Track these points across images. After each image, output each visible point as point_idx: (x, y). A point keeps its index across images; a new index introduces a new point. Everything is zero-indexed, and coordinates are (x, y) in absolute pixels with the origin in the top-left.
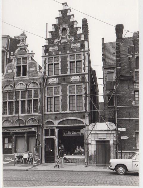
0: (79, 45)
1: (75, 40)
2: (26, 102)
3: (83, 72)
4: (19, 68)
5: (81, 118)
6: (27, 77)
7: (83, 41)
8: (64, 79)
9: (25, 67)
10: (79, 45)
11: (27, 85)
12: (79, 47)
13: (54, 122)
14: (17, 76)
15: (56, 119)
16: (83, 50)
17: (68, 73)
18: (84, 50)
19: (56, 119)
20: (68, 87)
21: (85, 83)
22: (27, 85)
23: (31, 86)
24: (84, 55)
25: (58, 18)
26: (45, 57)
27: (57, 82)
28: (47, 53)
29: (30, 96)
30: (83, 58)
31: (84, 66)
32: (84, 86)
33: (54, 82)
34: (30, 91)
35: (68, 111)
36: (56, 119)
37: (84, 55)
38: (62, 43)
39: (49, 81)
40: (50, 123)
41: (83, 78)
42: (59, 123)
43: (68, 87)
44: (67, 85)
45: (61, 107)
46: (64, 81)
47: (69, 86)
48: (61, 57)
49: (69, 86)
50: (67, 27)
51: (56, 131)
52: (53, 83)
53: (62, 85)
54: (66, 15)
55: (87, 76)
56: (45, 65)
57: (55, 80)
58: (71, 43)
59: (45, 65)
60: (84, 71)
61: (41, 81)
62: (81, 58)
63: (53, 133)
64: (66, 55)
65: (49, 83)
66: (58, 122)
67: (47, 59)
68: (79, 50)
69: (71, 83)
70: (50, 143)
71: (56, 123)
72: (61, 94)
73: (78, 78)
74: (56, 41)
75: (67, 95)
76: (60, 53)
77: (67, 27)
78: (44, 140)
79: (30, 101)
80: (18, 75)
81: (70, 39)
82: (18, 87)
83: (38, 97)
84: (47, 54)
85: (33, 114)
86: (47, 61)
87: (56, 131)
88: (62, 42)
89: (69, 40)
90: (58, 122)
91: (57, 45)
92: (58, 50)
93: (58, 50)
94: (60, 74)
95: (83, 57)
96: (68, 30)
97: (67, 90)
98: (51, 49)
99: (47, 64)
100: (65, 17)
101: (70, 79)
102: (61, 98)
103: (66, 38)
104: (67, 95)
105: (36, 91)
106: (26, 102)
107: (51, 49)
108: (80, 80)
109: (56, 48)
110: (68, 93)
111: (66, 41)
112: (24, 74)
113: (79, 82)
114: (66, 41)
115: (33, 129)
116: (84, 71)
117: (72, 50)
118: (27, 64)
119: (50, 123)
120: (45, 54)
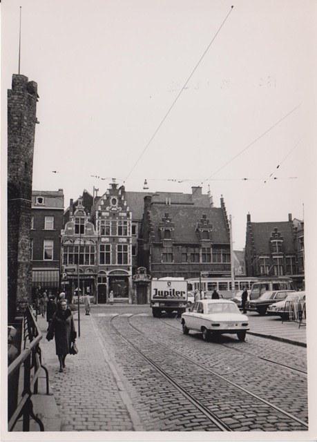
0: (125, 214)
2: (74, 256)
3: (128, 236)
4: (77, 226)
6: (84, 235)
7: (129, 212)
9: (82, 227)
10: (125, 214)
11: (85, 242)
13: (106, 272)
14: (76, 233)
15: (107, 270)
17: (117, 235)
22: (85, 242)
23: (88, 243)
25: (109, 190)
29: (87, 251)
34: (87, 247)
35: (117, 264)
40: (102, 272)
41: (128, 240)
42: (110, 273)
48: (112, 222)
51: (108, 278)
55: (131, 239)
57: (107, 239)
61: (97, 239)
63: (105, 281)
66: (109, 272)
68: (125, 218)
69: (119, 243)
70: (102, 288)
71: (107, 273)
73: (125, 240)
74: (108, 208)
78: (97, 287)
79: (87, 256)
80: (77, 232)
82: (77, 242)
83: (94, 251)
85: (90, 265)
87: (108, 278)
90: (109, 272)
94: (111, 235)
96: (117, 201)
98: (103, 214)
105: (93, 247)
106: (74, 256)
107: (103, 214)
109: (108, 214)
112: (82, 232)
113: (126, 243)
114: (115, 209)
115: (92, 277)
117: (120, 217)
118: (85, 224)
119: (102, 272)
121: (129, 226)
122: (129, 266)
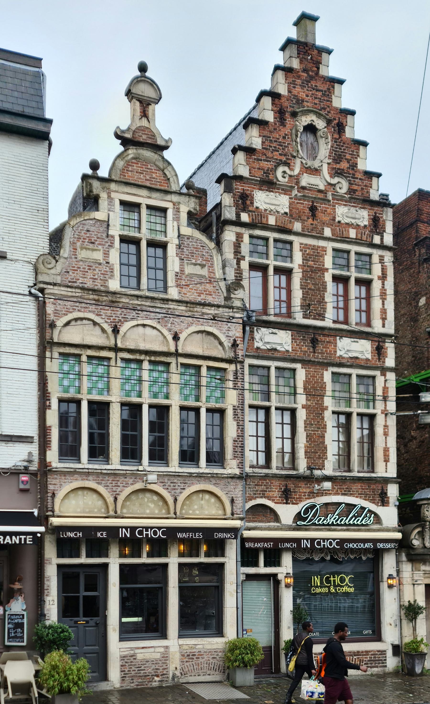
1: (351, 191)
5: (373, 501)
8: (314, 342)
12: (366, 223)
16: (377, 240)
18: (382, 239)
19: (287, 499)
20: (327, 376)
21: (384, 370)
24: (381, 259)
26: (238, 229)
27: (290, 350)
28: (244, 210)
30: (380, 274)
31: (383, 304)
32: (380, 381)
33: (279, 348)
36: (287, 499)
37: (381, 259)
38: (304, 188)
39: (257, 336)
43: (327, 376)
44: (327, 370)
45: (306, 452)
46: (314, 347)
47: (333, 373)
48: (304, 248)
49: (333, 373)
50: (320, 124)
52: (275, 350)
53: (305, 363)
54: (317, 73)
56: (238, 263)
58: (338, 198)
59: (238, 263)
60: (381, 321)
62: (370, 271)
64: (322, 243)
65: (256, 345)
67: (246, 239)
72: (304, 403)
75: (326, 408)
76: (297, 226)
77: (320, 124)
81: (334, 181)
84: (245, 217)
86: (245, 248)
88: (303, 183)
89: (330, 184)
91: (286, 190)
92: (287, 210)
93: (287, 210)
95: (377, 270)
97: (323, 387)
99: (247, 259)
100: (312, 78)
101: (336, 346)
102: (304, 418)
103: (316, 171)
104: (326, 408)
108: (370, 357)
110: (328, 402)
111: (322, 187)
116: (384, 326)
120: (238, 216)
121: (383, 277)
122: (386, 481)
